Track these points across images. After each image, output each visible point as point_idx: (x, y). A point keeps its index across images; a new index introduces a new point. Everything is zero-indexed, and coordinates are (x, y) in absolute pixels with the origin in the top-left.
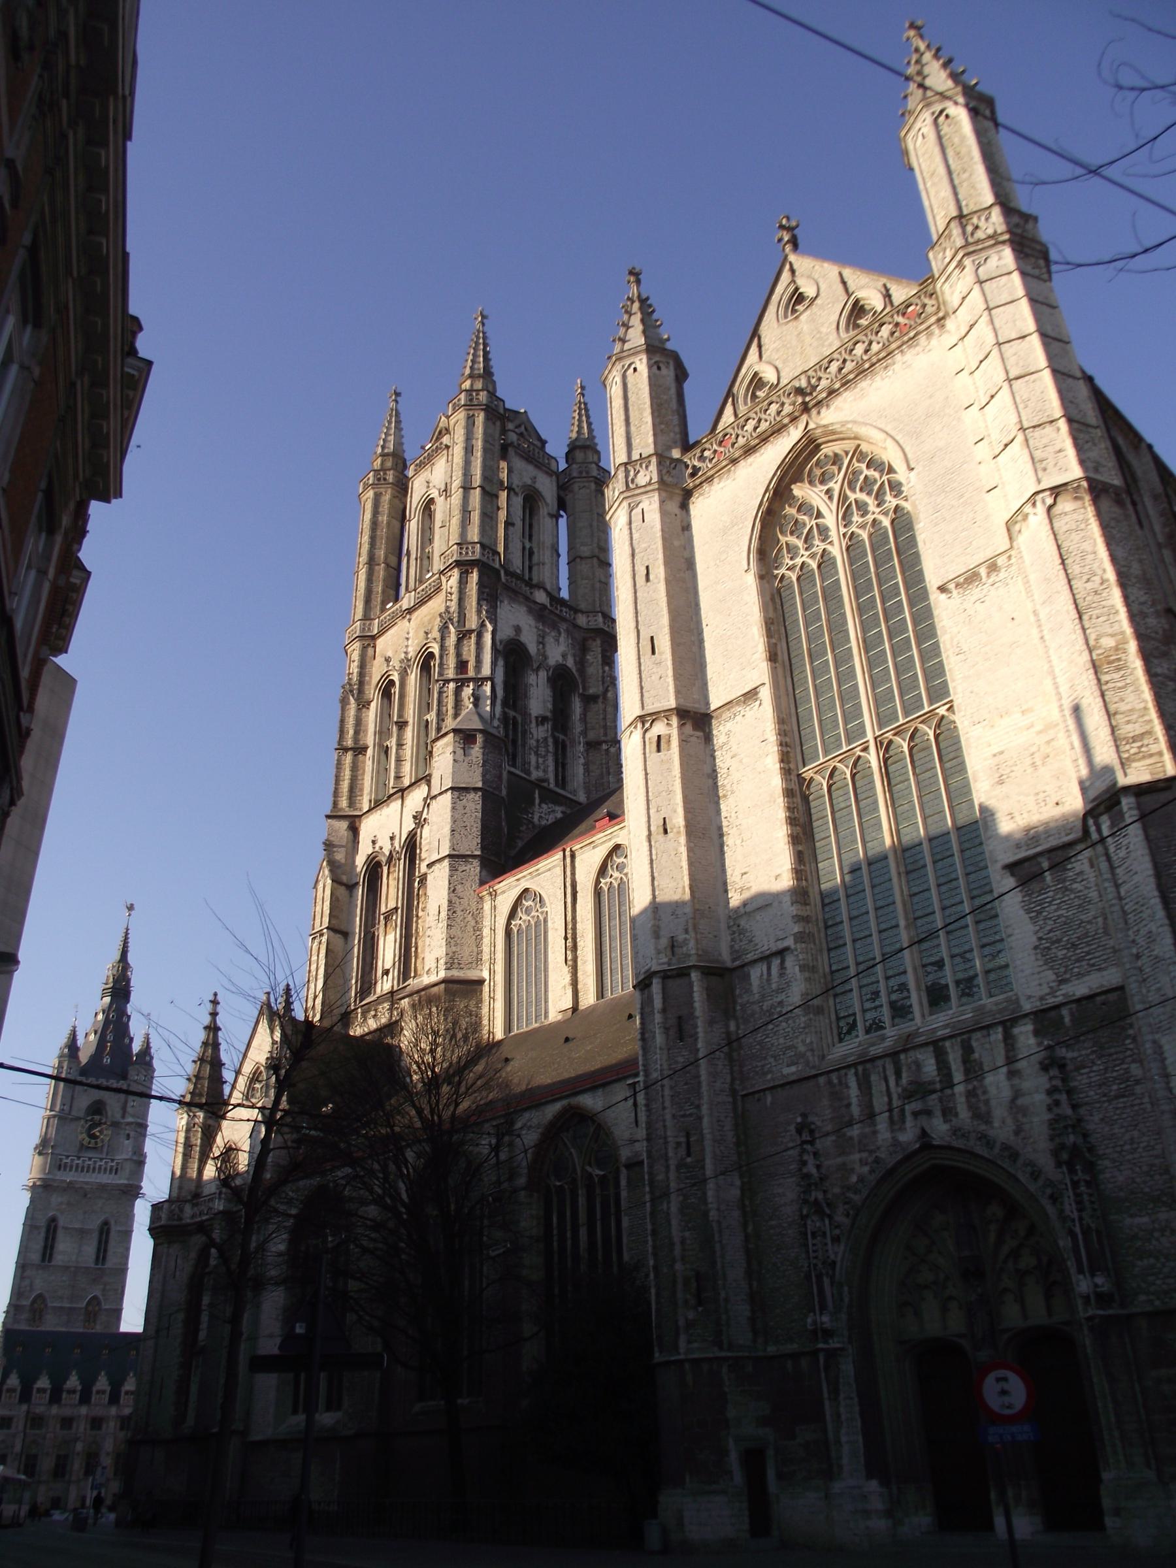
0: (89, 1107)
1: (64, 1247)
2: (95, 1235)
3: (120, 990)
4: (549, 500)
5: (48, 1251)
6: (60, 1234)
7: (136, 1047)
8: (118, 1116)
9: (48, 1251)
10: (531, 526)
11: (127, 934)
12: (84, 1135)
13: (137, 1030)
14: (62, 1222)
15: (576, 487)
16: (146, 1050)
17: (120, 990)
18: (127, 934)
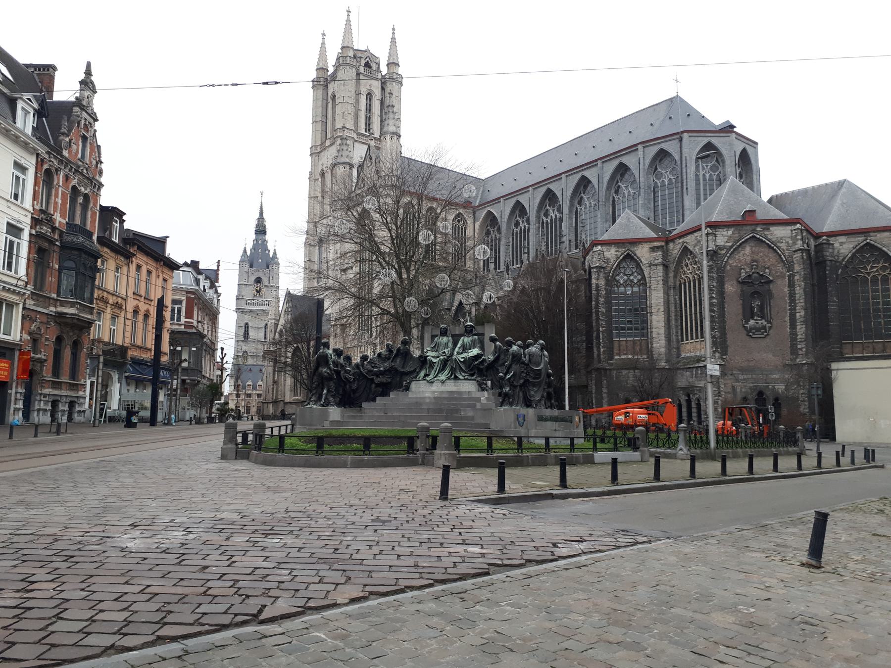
0: (255, 280)
1: (252, 333)
2: (264, 329)
3: (261, 230)
4: (377, 94)
5: (246, 335)
6: (250, 329)
7: (271, 255)
8: (267, 284)
9: (246, 335)
10: (370, 105)
11: (261, 205)
12: (255, 291)
13: (271, 247)
14: (250, 324)
15: (388, 84)
16: (275, 253)
17: (261, 230)
18: (261, 205)
